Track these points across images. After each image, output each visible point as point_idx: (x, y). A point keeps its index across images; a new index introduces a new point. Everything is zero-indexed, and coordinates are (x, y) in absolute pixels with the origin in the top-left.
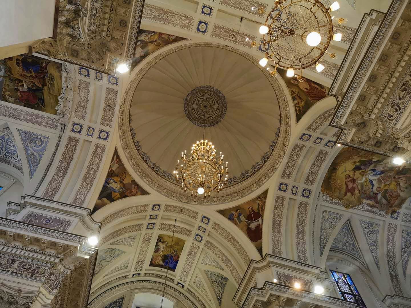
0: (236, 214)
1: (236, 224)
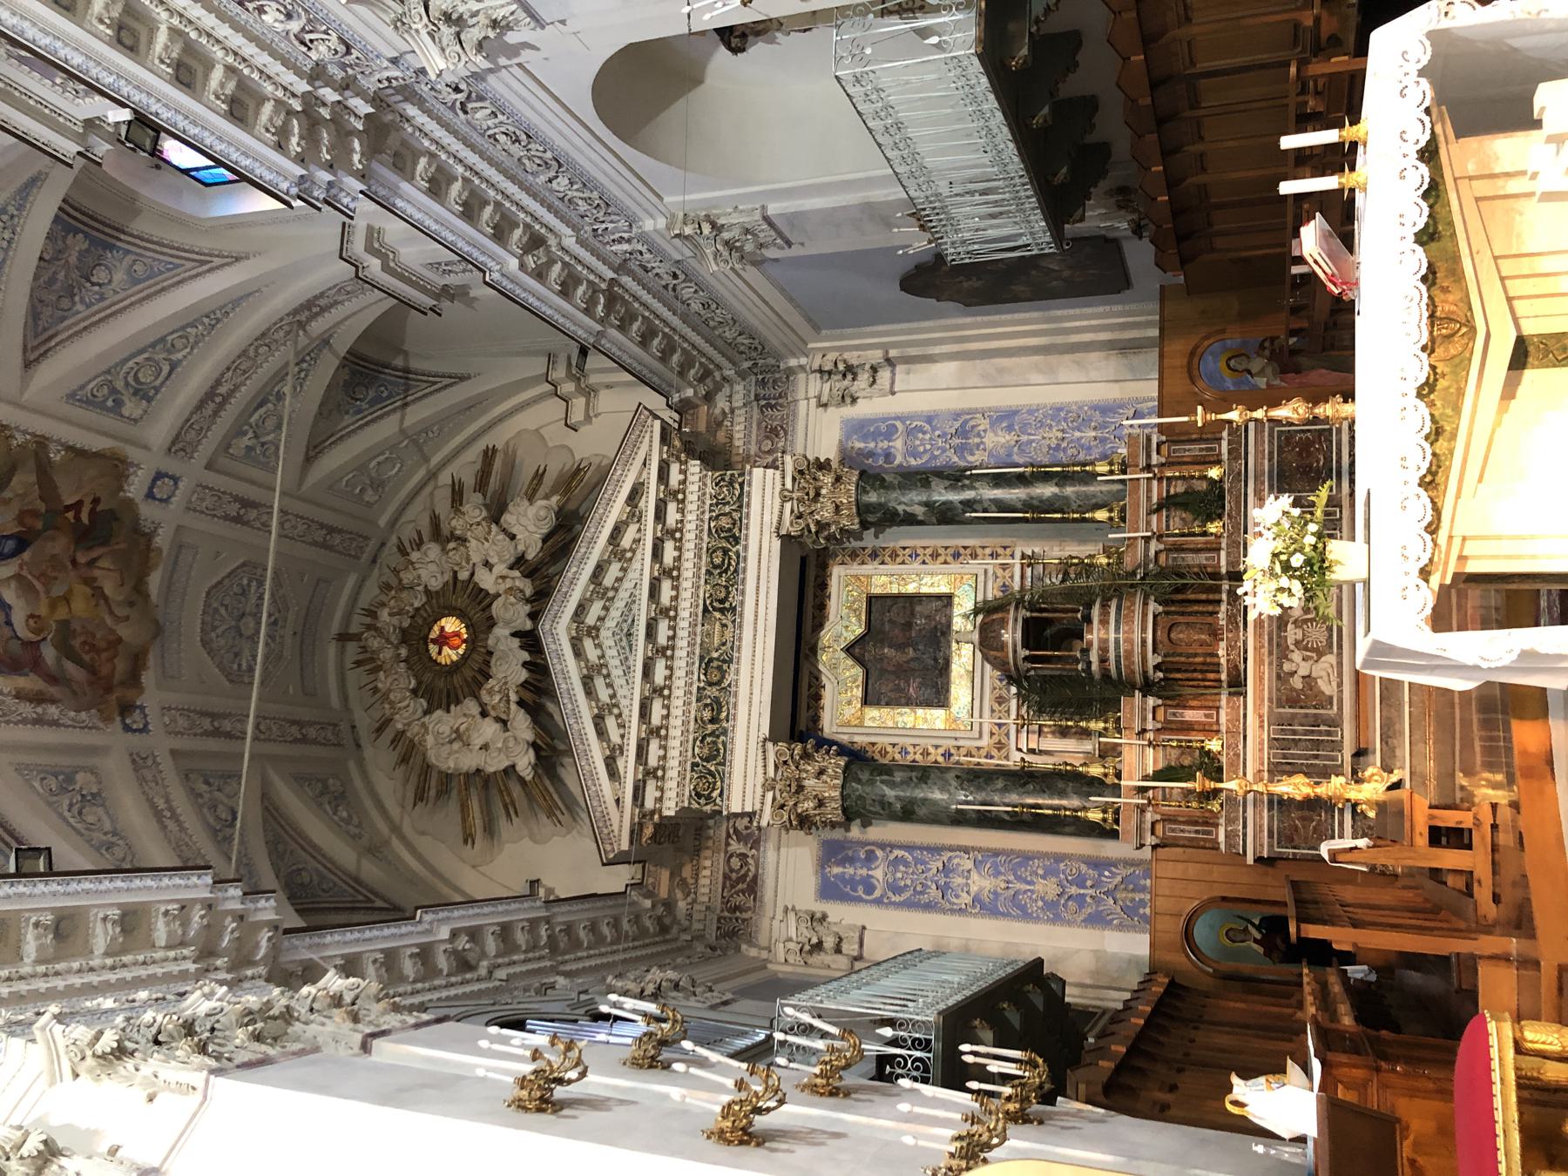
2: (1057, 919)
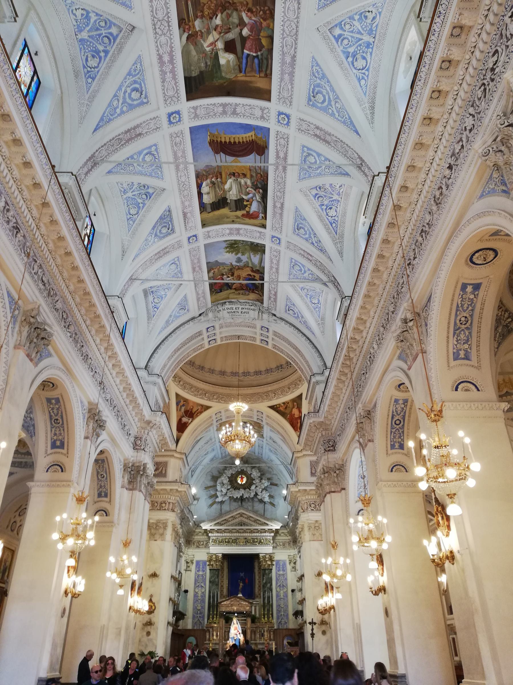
1: (177, 410)
2: (194, 609)
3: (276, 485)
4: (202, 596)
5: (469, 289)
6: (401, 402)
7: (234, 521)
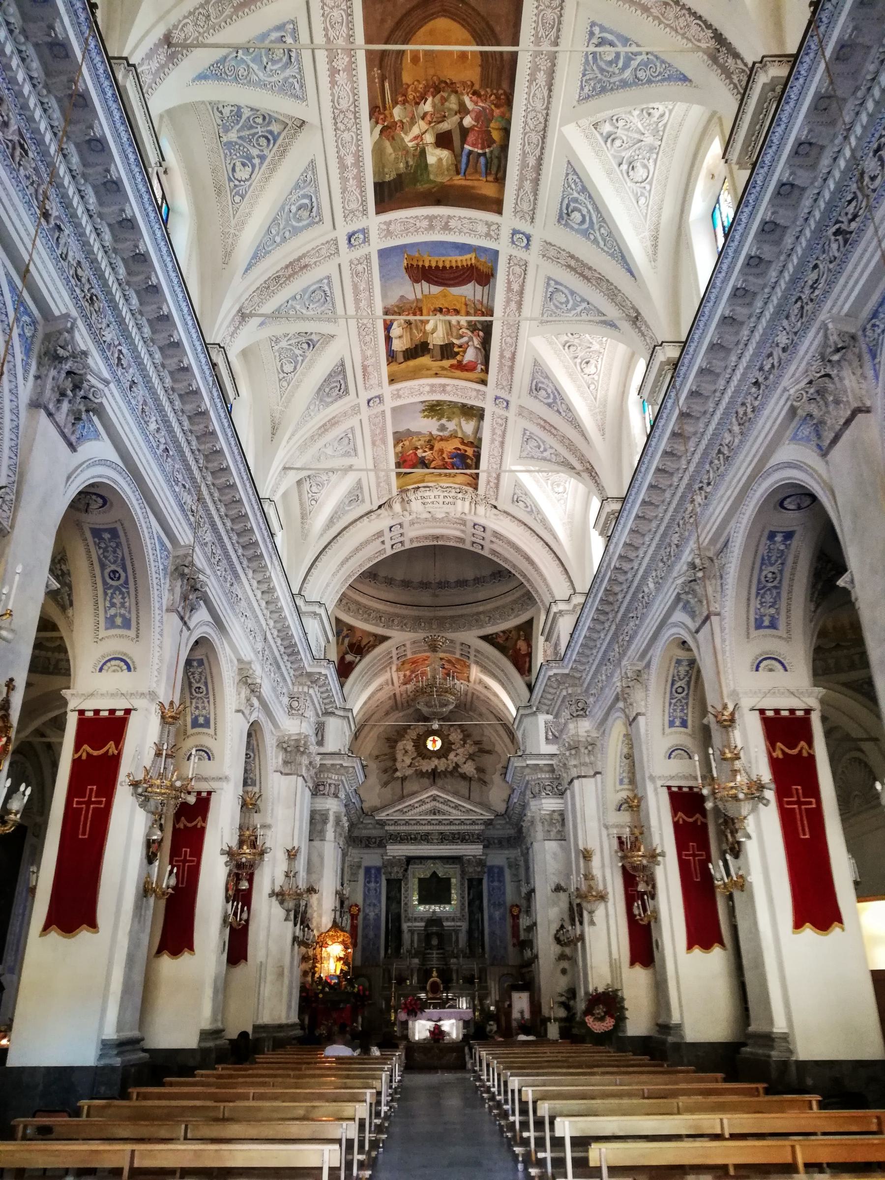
0: (345, 632)
3: (489, 752)
4: (375, 920)
5: (779, 538)
6: (685, 663)
7: (423, 808)
